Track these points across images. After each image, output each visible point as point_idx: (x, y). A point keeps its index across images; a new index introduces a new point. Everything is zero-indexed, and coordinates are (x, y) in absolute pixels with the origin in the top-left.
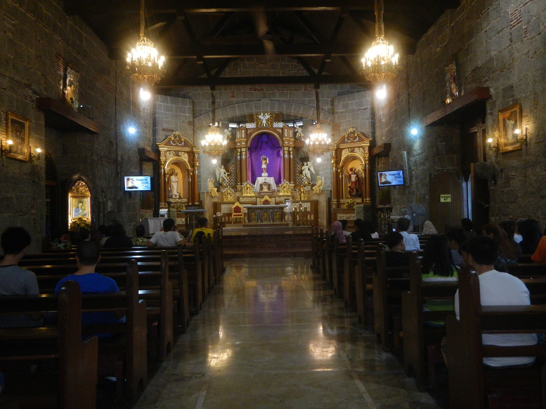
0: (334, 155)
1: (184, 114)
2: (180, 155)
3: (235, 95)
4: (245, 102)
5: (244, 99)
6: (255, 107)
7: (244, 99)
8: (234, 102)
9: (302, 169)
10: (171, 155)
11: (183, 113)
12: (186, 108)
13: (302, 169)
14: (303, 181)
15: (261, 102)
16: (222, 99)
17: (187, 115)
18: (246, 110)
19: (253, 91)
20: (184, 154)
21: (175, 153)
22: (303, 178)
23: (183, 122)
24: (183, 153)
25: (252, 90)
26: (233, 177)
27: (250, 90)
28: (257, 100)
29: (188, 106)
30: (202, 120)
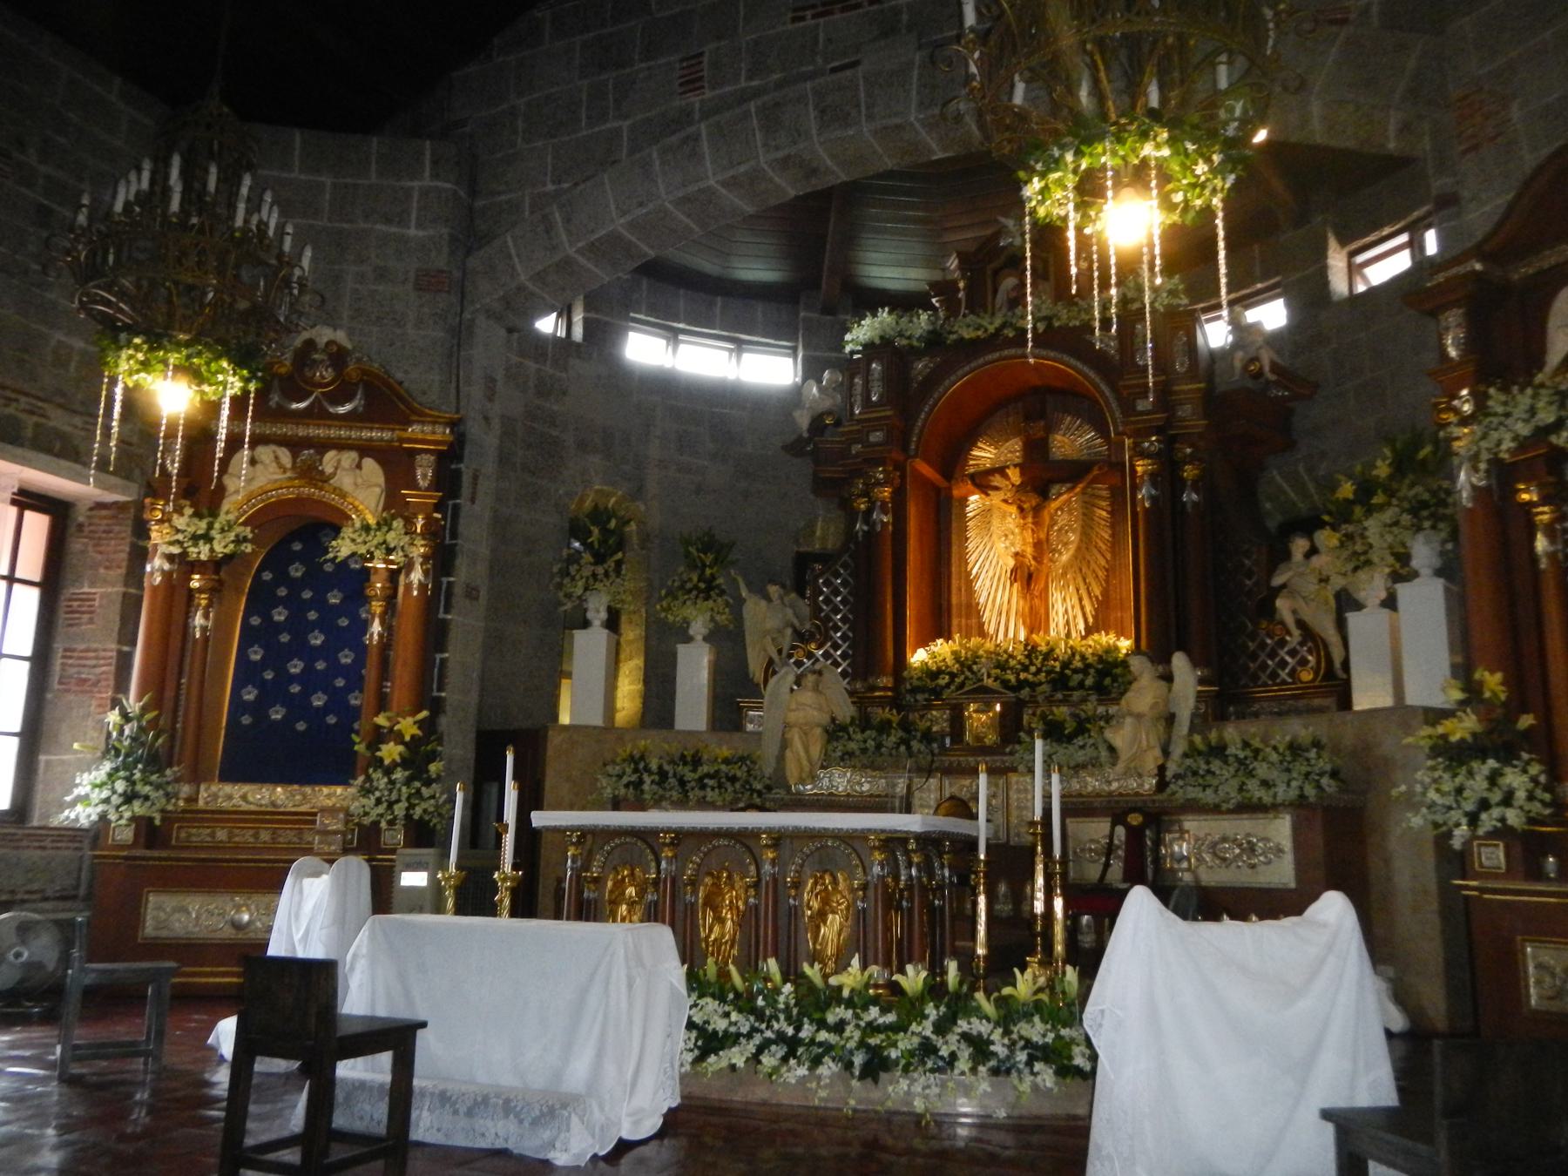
0: (1453, 353)
1: (393, 229)
2: (329, 469)
3: (705, 73)
4: (757, 93)
5: (755, 83)
6: (823, 112)
7: (755, 83)
8: (697, 116)
9: (1277, 581)
10: (259, 467)
11: (388, 221)
12: (408, 193)
13: (1277, 581)
14: (1283, 664)
15: (860, 69)
16: (626, 117)
17: (412, 232)
18: (765, 145)
19: (814, 17)
20: (359, 466)
21: (295, 456)
22: (1282, 643)
23: (382, 274)
24: (349, 457)
25: (809, 13)
26: (836, 647)
27: (794, 20)
28: (834, 70)
29: (426, 181)
30: (510, 257)
